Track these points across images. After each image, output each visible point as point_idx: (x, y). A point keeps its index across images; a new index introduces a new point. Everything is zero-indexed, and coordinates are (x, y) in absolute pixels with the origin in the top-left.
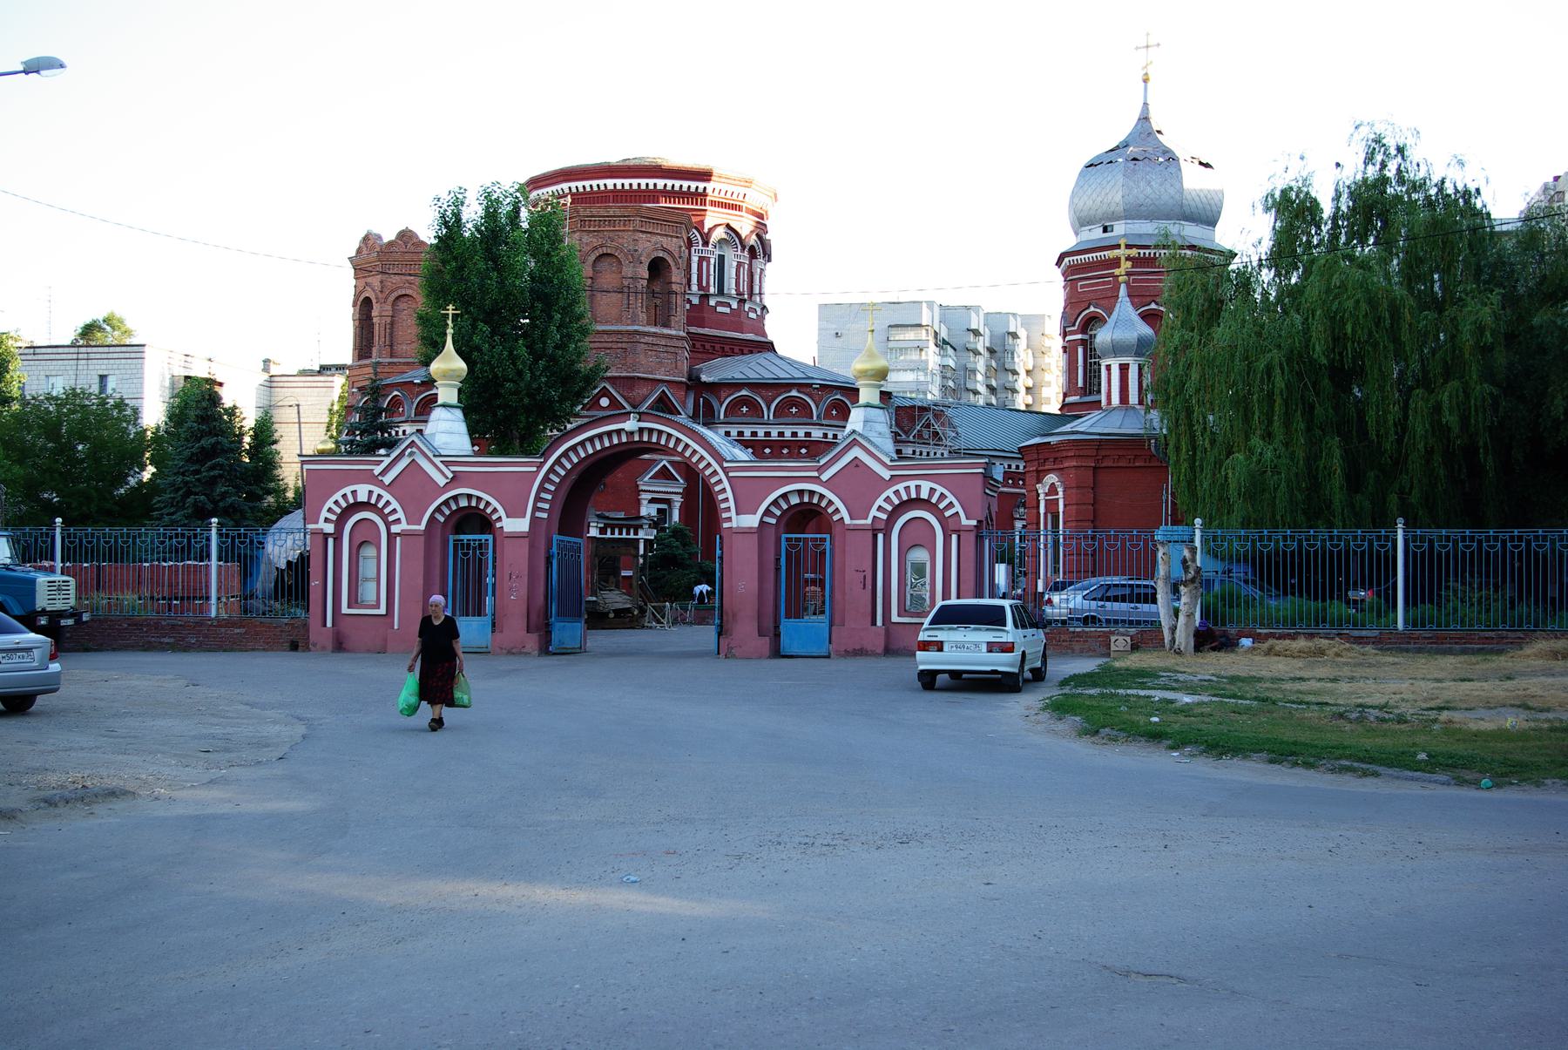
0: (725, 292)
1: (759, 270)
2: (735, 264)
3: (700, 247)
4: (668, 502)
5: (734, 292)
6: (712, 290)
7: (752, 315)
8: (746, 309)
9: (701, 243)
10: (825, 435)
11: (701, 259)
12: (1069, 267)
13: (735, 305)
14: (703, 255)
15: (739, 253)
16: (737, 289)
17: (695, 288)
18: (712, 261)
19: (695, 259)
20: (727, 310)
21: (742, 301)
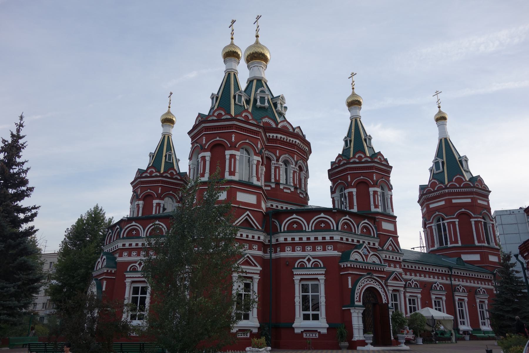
0: (288, 184)
1: (304, 178)
2: (292, 172)
3: (275, 162)
4: (251, 278)
5: (292, 184)
6: (281, 182)
7: (301, 195)
8: (298, 192)
9: (275, 160)
10: (342, 239)
11: (276, 168)
12: (425, 199)
13: (292, 189)
14: (277, 166)
15: (294, 166)
16: (294, 183)
17: (273, 180)
18: (281, 169)
19: (273, 168)
20: (289, 191)
21: (296, 188)
